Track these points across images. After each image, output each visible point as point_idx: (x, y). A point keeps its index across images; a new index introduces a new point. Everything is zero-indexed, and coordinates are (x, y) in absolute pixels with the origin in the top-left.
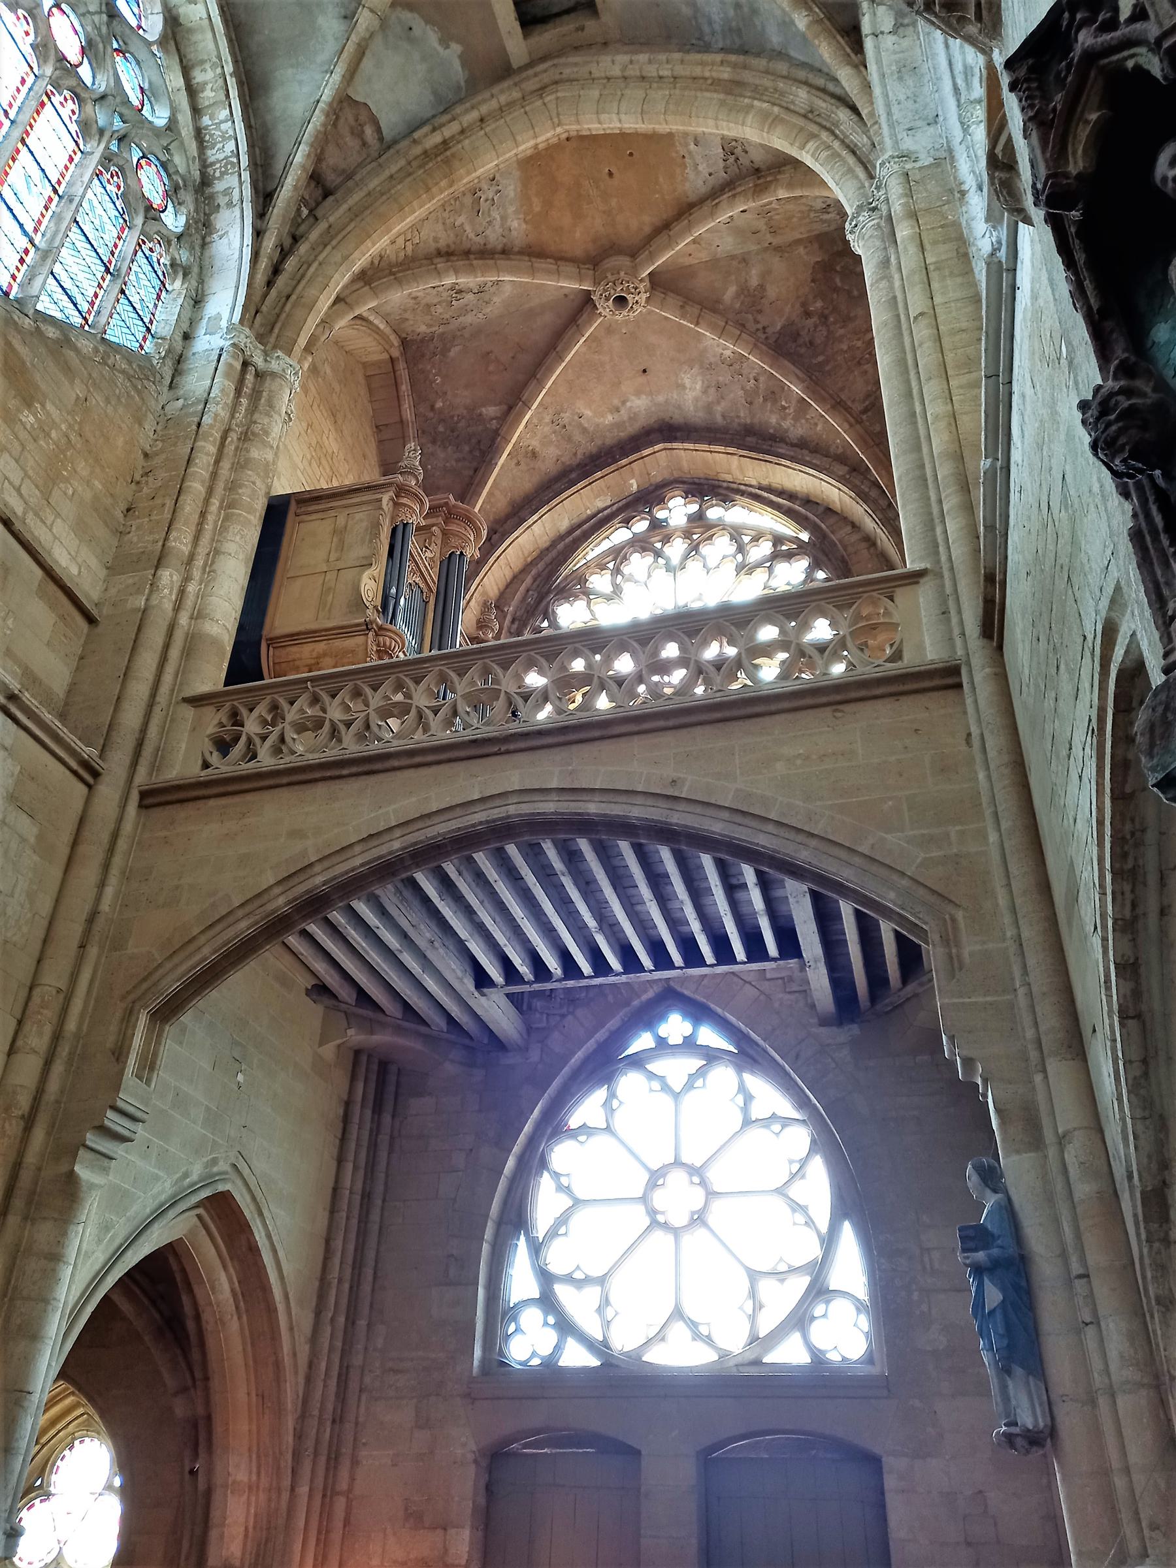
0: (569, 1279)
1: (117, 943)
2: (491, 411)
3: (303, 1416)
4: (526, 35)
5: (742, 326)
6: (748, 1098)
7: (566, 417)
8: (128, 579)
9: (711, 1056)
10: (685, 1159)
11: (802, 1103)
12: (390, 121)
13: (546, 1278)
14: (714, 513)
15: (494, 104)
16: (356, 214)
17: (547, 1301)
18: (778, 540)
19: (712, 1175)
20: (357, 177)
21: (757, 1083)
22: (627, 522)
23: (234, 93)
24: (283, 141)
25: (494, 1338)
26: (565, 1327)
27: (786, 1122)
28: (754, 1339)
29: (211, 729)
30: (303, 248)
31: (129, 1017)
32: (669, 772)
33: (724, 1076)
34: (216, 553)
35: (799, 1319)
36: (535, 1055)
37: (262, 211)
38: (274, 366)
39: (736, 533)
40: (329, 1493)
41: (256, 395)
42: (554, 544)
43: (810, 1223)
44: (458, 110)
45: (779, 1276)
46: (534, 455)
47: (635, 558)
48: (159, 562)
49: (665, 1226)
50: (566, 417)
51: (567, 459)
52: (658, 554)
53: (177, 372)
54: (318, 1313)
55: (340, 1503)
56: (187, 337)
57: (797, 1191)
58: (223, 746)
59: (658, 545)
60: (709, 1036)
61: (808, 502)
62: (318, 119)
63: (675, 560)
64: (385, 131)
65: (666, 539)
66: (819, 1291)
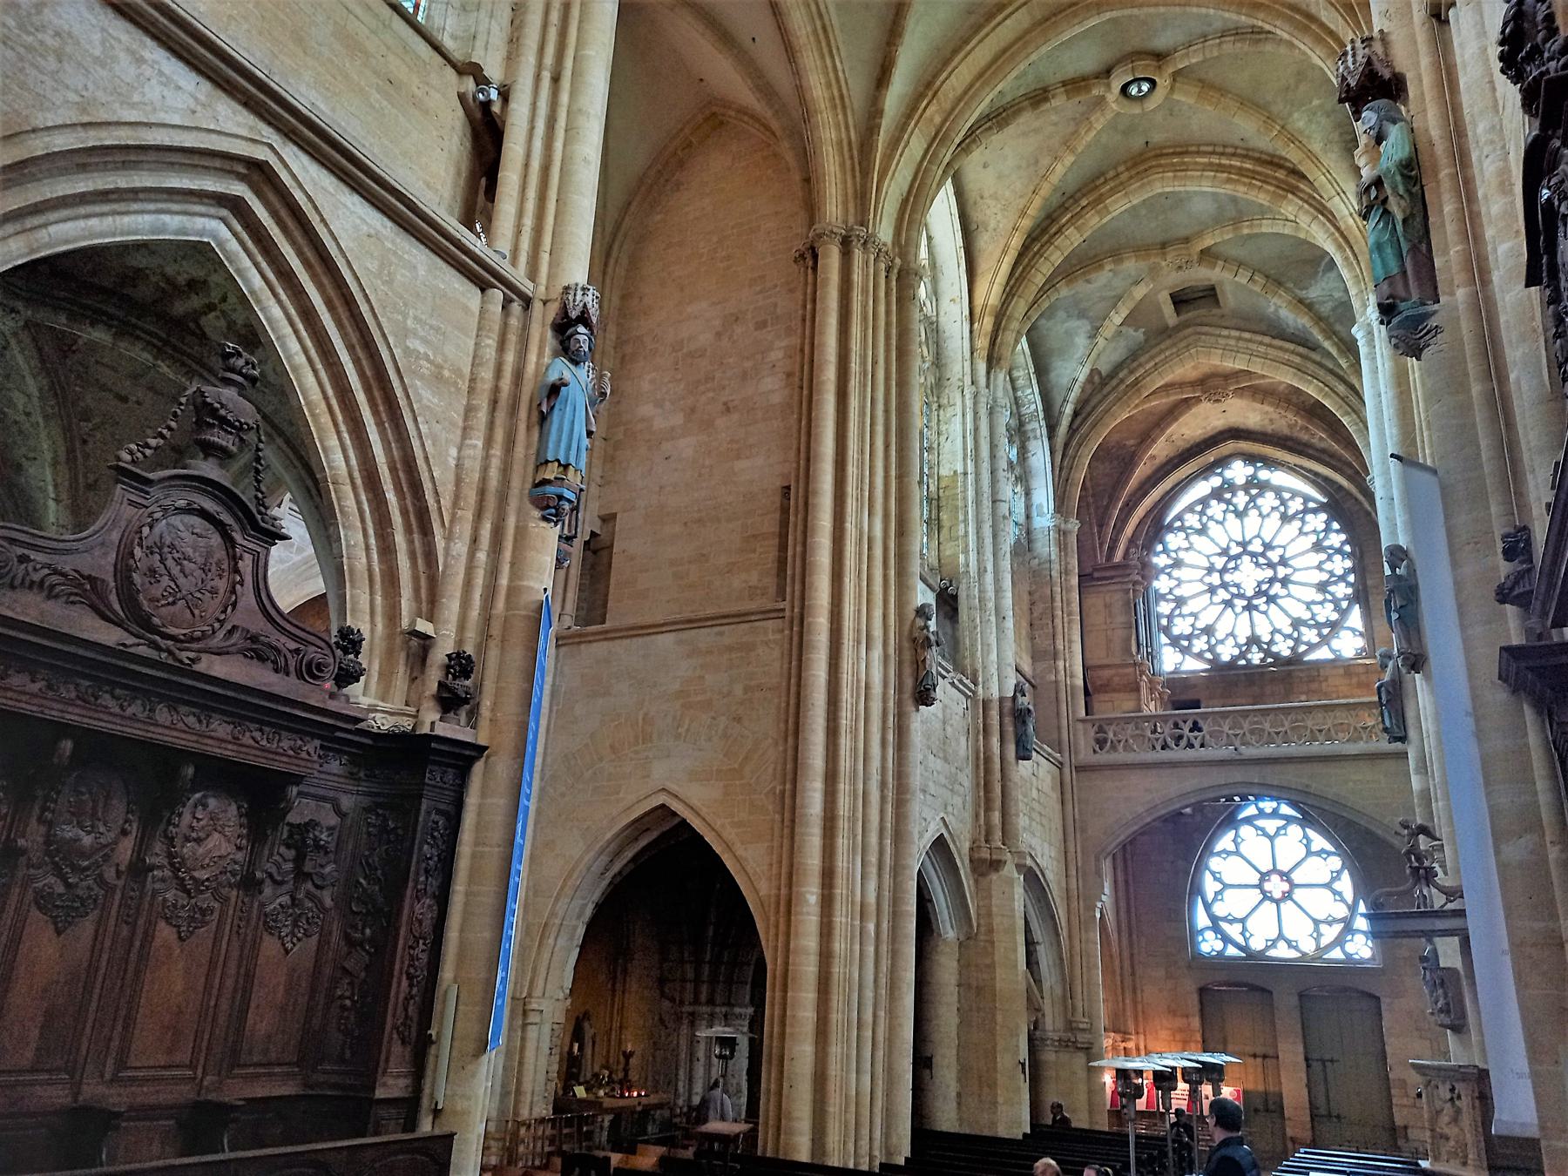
0: (1225, 919)
1: (1083, 831)
2: (1132, 442)
3: (1121, 975)
4: (1178, 312)
5: (1288, 402)
6: (1309, 841)
7: (1174, 437)
8: (1041, 666)
9: (1289, 819)
10: (1279, 867)
11: (1337, 846)
12: (1104, 368)
13: (1215, 920)
14: (1264, 475)
15: (1163, 356)
16: (1094, 426)
17: (1215, 928)
18: (1307, 499)
19: (1293, 876)
20: (1092, 403)
21: (1311, 833)
22: (1206, 479)
23: (1034, 381)
24: (1058, 400)
25: (1195, 944)
26: (1226, 939)
27: (1329, 854)
28: (1318, 948)
29: (1092, 734)
30: (1071, 452)
31: (1097, 859)
32: (1305, 781)
33: (1295, 831)
34: (1070, 642)
35: (1339, 941)
36: (1198, 818)
37: (1051, 435)
38: (1069, 526)
39: (1278, 491)
40: (1135, 1002)
41: (1066, 544)
42: (1162, 498)
43: (1343, 900)
44: (1142, 359)
45: (1330, 922)
46: (1153, 457)
47: (1214, 503)
48: (1055, 658)
49: (1272, 900)
50: (1174, 437)
51: (1172, 455)
52: (1228, 502)
53: (1030, 541)
54: (1119, 934)
55: (1140, 1007)
56: (1028, 517)
57: (1337, 886)
58: (1101, 743)
59: (1228, 496)
60: (1285, 809)
61: (1326, 479)
62: (1077, 390)
63: (1241, 508)
64: (1104, 374)
65: (1234, 495)
66: (1348, 928)
